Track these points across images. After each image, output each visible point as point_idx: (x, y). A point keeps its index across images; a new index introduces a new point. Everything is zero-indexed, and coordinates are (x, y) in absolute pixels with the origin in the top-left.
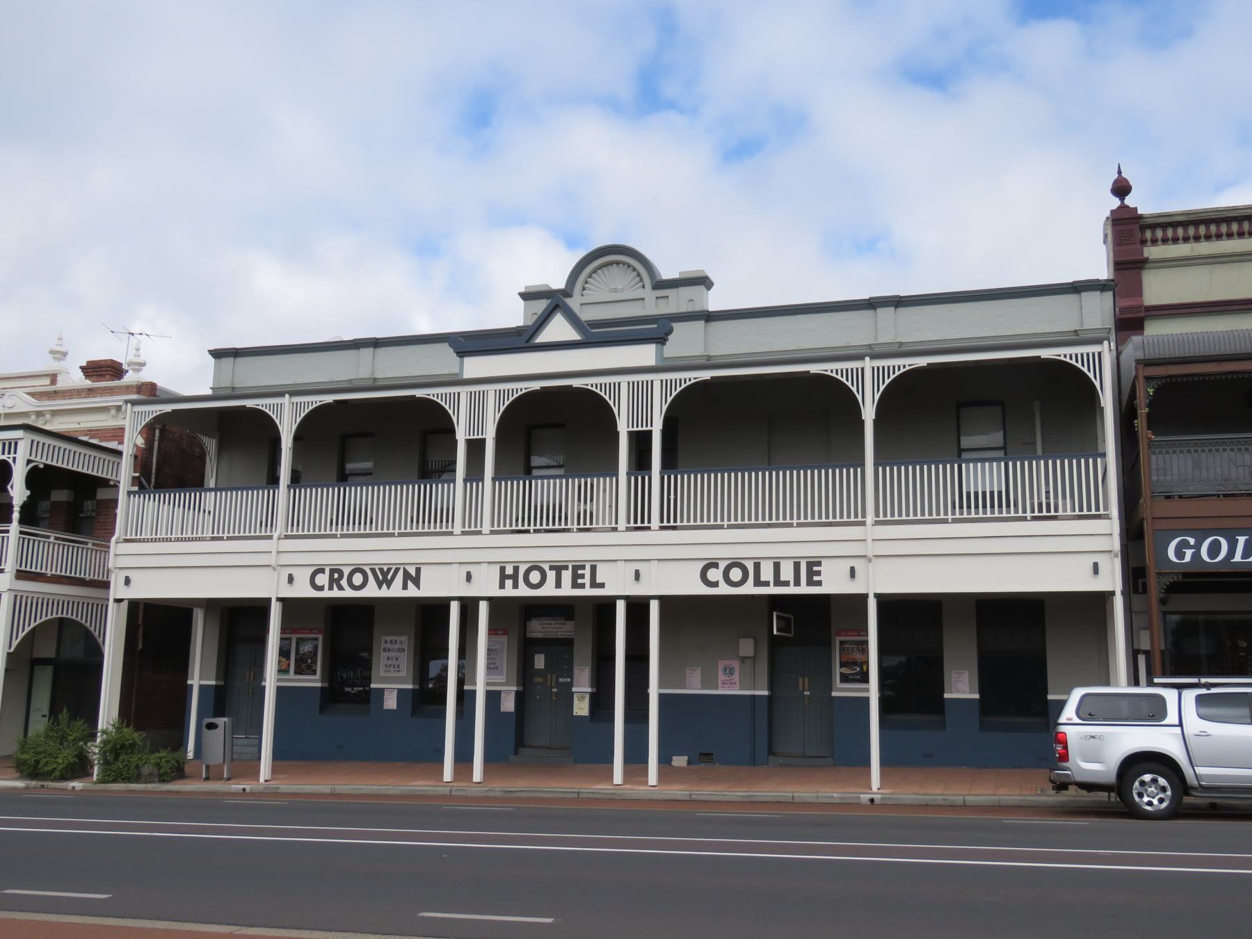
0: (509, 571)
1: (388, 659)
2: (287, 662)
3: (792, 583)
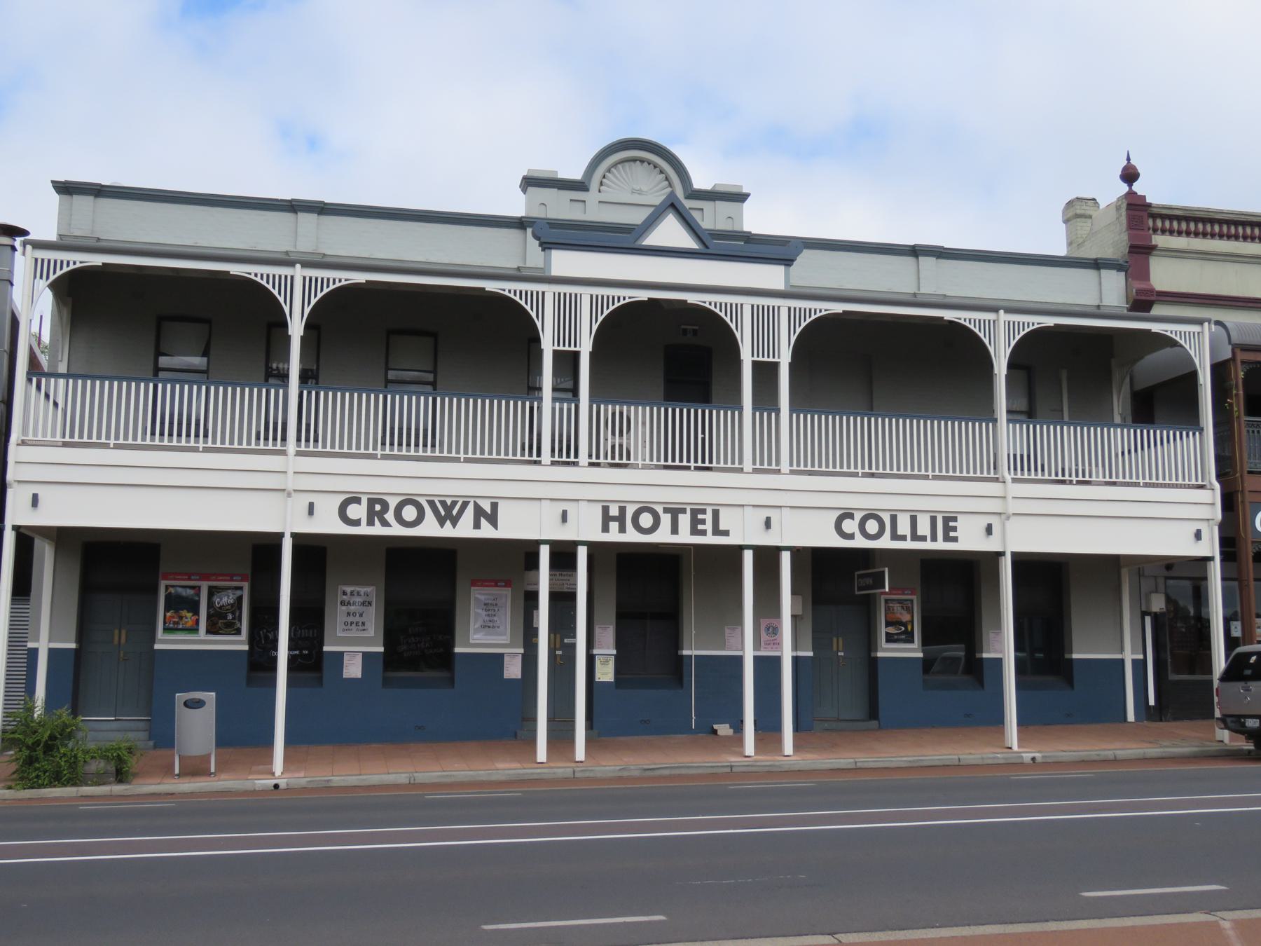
0: (614, 511)
1: (349, 614)
2: (195, 618)
3: (929, 538)
